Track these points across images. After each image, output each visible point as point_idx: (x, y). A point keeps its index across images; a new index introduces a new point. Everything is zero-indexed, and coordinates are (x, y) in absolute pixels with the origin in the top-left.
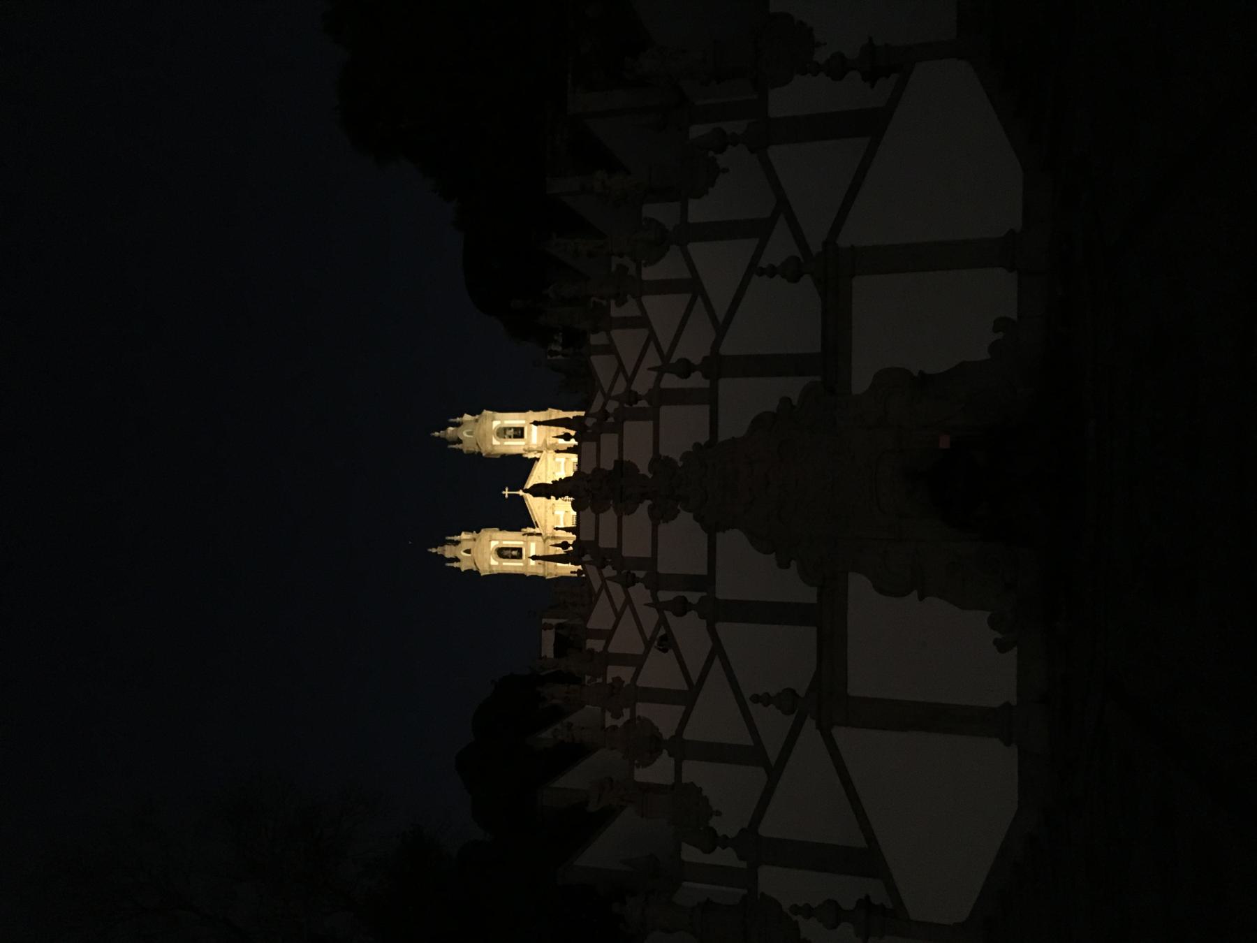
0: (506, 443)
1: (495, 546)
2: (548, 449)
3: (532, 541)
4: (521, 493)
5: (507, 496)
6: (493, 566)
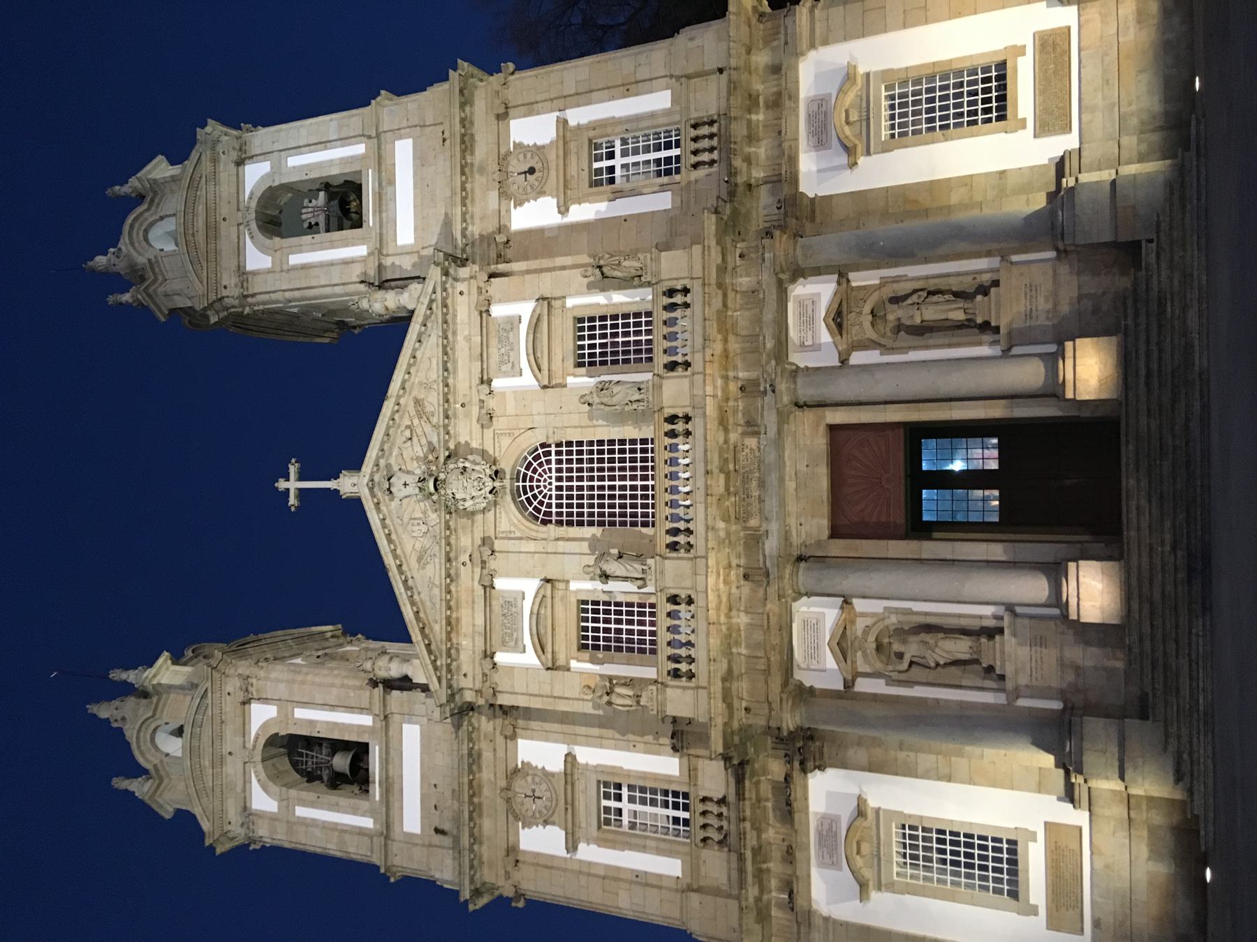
0: (295, 259)
1: (265, 725)
2: (463, 262)
3: (410, 716)
4: (347, 484)
5: (292, 500)
6: (261, 815)
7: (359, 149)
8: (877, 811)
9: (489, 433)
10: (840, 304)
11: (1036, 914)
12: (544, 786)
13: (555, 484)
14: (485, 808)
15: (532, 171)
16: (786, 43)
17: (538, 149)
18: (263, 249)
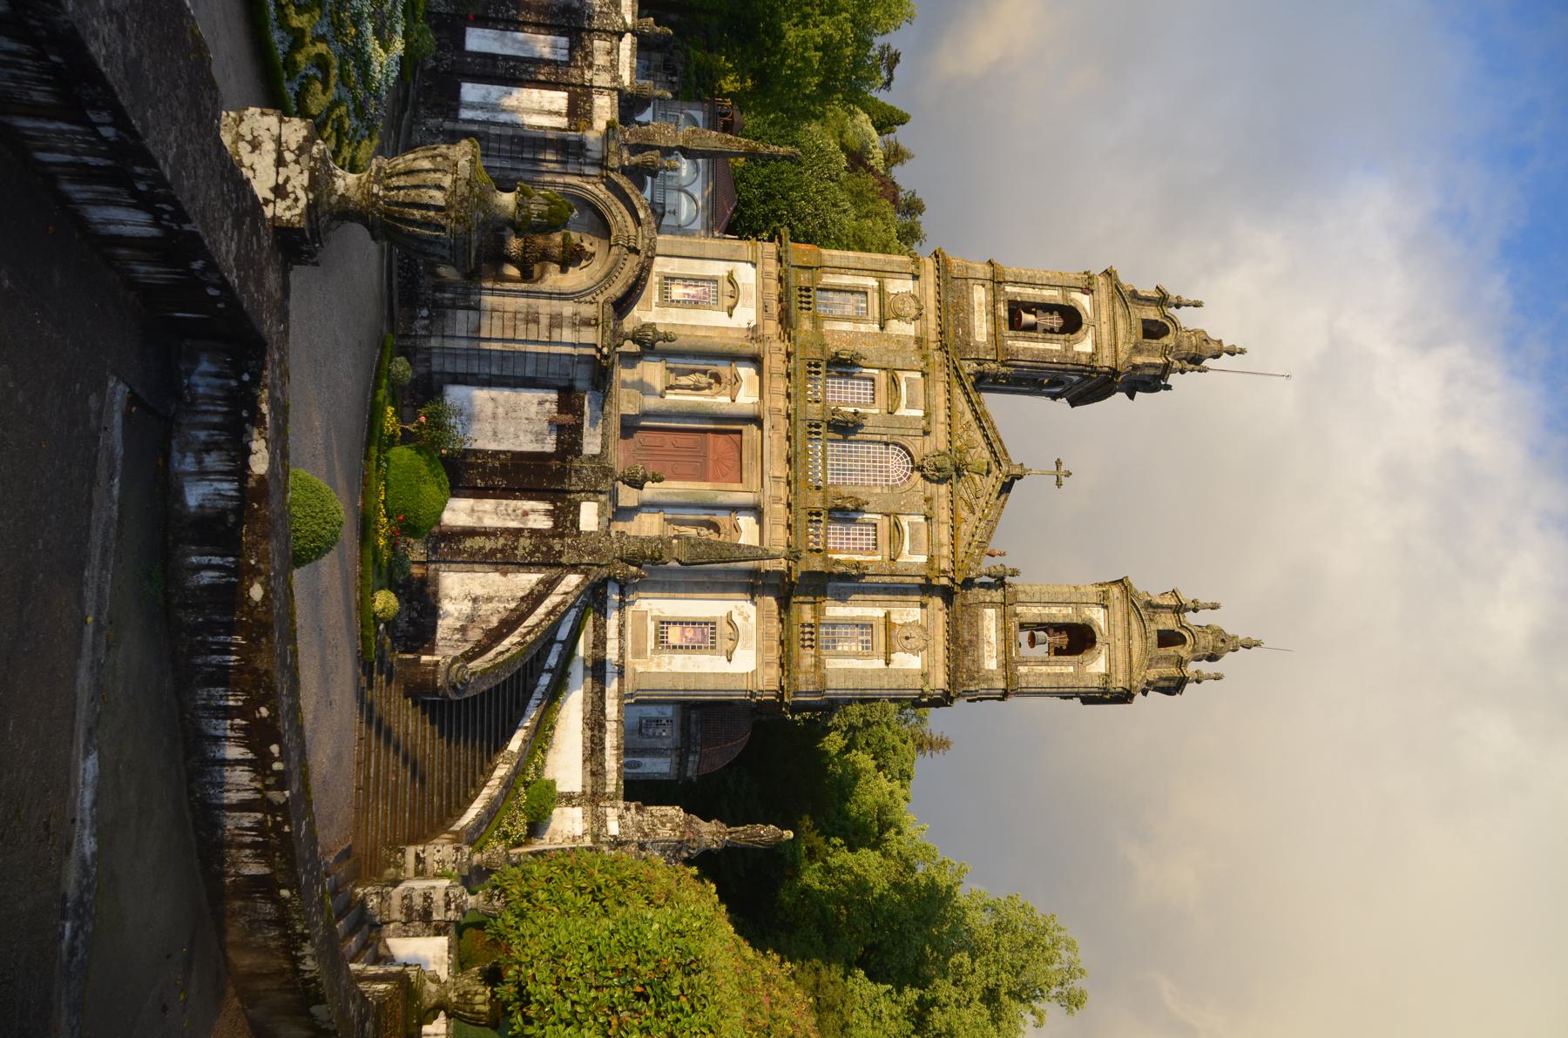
9: (928, 495)
15: (907, 638)
17: (904, 650)
18: (1091, 620)
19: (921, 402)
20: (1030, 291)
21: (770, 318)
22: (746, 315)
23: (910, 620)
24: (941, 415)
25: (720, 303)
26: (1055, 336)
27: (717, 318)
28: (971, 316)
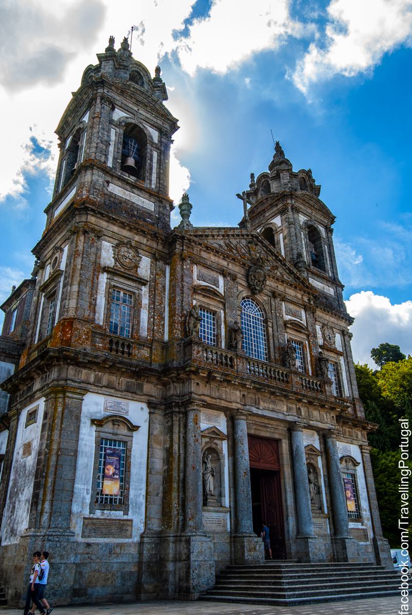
7: (330, 275)
8: (132, 437)
9: (269, 294)
10: (315, 452)
11: (90, 513)
12: (133, 265)
13: (252, 315)
14: (122, 230)
15: (330, 338)
16: (363, 441)
18: (305, 223)
19: (214, 274)
20: (111, 149)
21: (140, 387)
22: (137, 412)
23: (320, 333)
24: (225, 263)
25: (125, 439)
26: (148, 150)
27: (139, 444)
28: (135, 205)
